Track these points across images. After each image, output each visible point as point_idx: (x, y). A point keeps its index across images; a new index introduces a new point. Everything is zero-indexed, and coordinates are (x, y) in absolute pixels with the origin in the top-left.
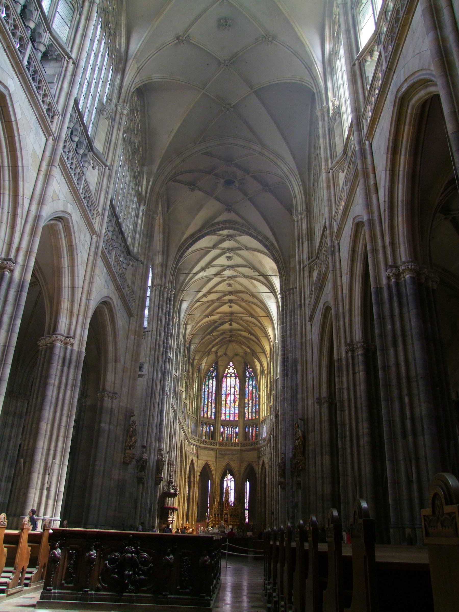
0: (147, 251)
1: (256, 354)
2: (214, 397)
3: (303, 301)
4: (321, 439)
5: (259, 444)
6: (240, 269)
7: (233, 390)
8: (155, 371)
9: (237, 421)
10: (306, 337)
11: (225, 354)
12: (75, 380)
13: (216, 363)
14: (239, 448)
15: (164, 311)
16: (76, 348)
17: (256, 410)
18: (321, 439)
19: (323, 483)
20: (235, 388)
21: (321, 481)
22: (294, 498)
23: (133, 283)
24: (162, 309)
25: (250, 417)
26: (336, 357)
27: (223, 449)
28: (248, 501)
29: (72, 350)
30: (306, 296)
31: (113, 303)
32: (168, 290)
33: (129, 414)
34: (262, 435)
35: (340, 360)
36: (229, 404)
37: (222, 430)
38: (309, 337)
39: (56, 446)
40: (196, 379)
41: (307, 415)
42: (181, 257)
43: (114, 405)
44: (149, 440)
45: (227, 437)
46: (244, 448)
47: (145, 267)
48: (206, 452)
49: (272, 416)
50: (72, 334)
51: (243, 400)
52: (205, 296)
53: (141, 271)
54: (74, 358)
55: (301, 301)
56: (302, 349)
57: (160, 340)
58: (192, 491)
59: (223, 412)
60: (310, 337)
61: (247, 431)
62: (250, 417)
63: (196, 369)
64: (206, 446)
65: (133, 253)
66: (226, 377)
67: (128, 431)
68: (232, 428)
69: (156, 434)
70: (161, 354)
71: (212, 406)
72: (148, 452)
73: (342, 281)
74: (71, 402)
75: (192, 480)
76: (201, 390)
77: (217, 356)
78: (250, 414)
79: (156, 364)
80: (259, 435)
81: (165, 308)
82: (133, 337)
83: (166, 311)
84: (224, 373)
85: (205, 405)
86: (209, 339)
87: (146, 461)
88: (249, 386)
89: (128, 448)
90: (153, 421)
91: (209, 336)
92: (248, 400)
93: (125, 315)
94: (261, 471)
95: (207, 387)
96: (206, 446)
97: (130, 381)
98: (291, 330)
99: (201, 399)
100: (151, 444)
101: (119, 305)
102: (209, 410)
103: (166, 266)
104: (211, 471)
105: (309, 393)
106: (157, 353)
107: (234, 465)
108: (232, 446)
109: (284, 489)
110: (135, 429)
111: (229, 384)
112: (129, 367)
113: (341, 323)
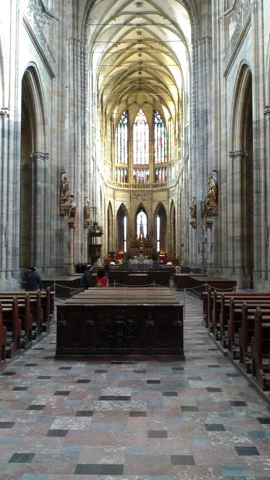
0: (61, 6)
1: (165, 102)
3: (218, 56)
4: (233, 189)
6: (149, 16)
7: (143, 136)
8: (76, 126)
9: (148, 165)
10: (220, 93)
11: (136, 102)
12: (16, 149)
13: (127, 112)
14: (151, 189)
15: (79, 65)
16: (12, 118)
18: (233, 189)
19: (233, 227)
21: (231, 225)
22: (204, 235)
23: (51, 42)
24: (77, 64)
25: (160, 162)
26: (254, 119)
27: (137, 191)
29: (9, 121)
30: (221, 50)
31: (37, 66)
32: (82, 43)
33: (60, 172)
34: (171, 177)
35: (258, 122)
38: (223, 93)
39: (8, 210)
40: (109, 127)
41: (220, 167)
42: (91, 6)
43: (47, 165)
44: (76, 190)
45: (139, 180)
46: (154, 189)
47: (61, 25)
49: (181, 161)
50: (6, 106)
51: (153, 146)
52: (115, 45)
53: (57, 29)
54: (12, 129)
55: (216, 55)
56: (216, 104)
57: (77, 95)
58: (110, 227)
60: (225, 93)
61: (157, 174)
63: (108, 118)
64: (121, 188)
65: (47, 9)
66: (136, 123)
67: (61, 187)
69: (81, 184)
70: (80, 109)
72: (76, 200)
73: (263, 42)
74: (15, 170)
77: (127, 104)
79: (76, 119)
80: (168, 177)
81: (79, 63)
82: (56, 98)
83: (81, 66)
86: (120, 88)
87: (75, 209)
89: (63, 201)
90: (78, 172)
91: (119, 86)
93: (48, 76)
96: (121, 188)
97: (58, 141)
98: (202, 80)
99: (114, 146)
100: (77, 193)
101: (42, 68)
103: (77, 17)
105: (222, 146)
106: (76, 108)
108: (144, 187)
109: (195, 228)
110: (67, 185)
112: (56, 128)
113: (261, 86)
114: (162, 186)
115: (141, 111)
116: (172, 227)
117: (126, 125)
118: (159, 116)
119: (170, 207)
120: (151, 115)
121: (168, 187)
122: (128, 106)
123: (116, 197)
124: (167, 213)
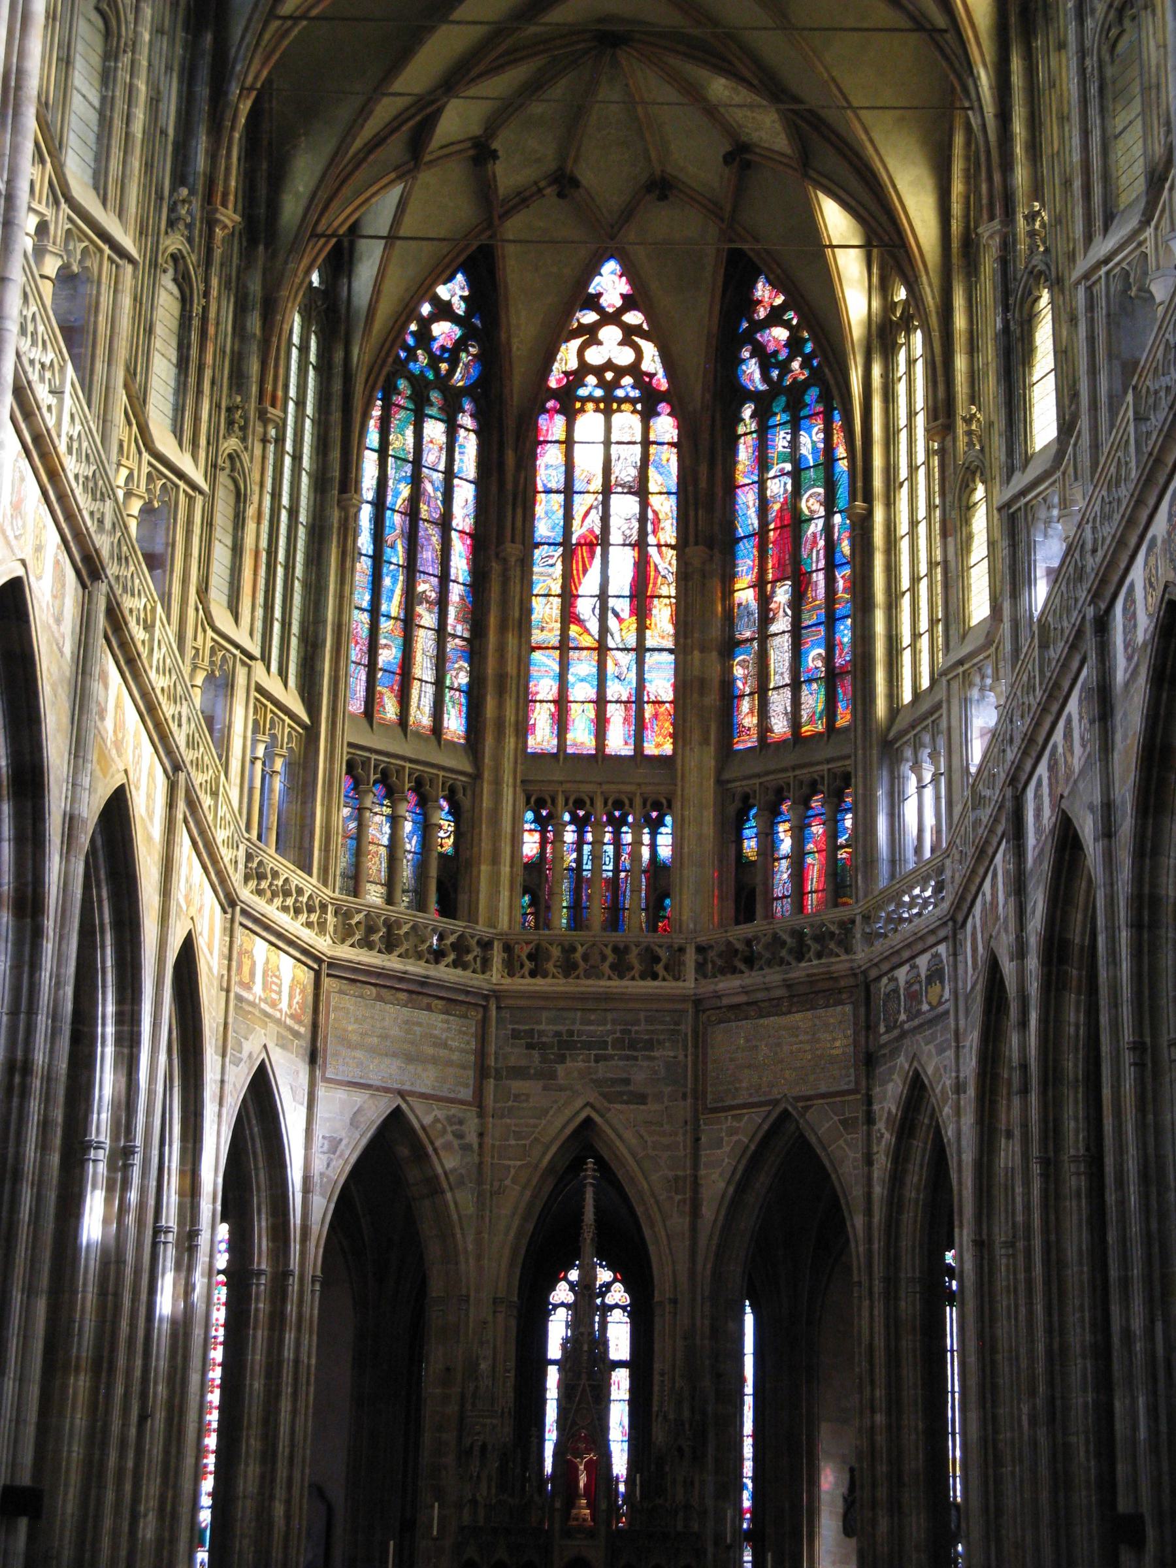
2: (460, 565)
7: (624, 507)
11: (564, 182)
14: (689, 984)
17: (829, 659)
20: (641, 490)
25: (780, 726)
28: (748, 1468)
36: (593, 626)
37: (530, 845)
45: (576, 908)
48: (392, 1016)
58: (257, 1356)
59: (544, 687)
61: (750, 846)
62: (780, 726)
64: (392, 962)
75: (262, 1262)
76: (349, 481)
77: (484, 191)
84: (546, 370)
85: (385, 625)
92: (761, 585)
94: (896, 1179)
95: (398, 474)
96: (392, 962)
102: (423, 669)
104: (433, 1187)
107: (639, 1141)
108: (620, 969)
111: (588, 461)
114: (800, 954)
115: (610, 284)
116: (911, 1375)
117: (468, 406)
118: (781, 334)
119: (882, 1162)
120: (699, 315)
121: (861, 954)
122: (491, 206)
123: (331, 1045)
124: (859, 1221)
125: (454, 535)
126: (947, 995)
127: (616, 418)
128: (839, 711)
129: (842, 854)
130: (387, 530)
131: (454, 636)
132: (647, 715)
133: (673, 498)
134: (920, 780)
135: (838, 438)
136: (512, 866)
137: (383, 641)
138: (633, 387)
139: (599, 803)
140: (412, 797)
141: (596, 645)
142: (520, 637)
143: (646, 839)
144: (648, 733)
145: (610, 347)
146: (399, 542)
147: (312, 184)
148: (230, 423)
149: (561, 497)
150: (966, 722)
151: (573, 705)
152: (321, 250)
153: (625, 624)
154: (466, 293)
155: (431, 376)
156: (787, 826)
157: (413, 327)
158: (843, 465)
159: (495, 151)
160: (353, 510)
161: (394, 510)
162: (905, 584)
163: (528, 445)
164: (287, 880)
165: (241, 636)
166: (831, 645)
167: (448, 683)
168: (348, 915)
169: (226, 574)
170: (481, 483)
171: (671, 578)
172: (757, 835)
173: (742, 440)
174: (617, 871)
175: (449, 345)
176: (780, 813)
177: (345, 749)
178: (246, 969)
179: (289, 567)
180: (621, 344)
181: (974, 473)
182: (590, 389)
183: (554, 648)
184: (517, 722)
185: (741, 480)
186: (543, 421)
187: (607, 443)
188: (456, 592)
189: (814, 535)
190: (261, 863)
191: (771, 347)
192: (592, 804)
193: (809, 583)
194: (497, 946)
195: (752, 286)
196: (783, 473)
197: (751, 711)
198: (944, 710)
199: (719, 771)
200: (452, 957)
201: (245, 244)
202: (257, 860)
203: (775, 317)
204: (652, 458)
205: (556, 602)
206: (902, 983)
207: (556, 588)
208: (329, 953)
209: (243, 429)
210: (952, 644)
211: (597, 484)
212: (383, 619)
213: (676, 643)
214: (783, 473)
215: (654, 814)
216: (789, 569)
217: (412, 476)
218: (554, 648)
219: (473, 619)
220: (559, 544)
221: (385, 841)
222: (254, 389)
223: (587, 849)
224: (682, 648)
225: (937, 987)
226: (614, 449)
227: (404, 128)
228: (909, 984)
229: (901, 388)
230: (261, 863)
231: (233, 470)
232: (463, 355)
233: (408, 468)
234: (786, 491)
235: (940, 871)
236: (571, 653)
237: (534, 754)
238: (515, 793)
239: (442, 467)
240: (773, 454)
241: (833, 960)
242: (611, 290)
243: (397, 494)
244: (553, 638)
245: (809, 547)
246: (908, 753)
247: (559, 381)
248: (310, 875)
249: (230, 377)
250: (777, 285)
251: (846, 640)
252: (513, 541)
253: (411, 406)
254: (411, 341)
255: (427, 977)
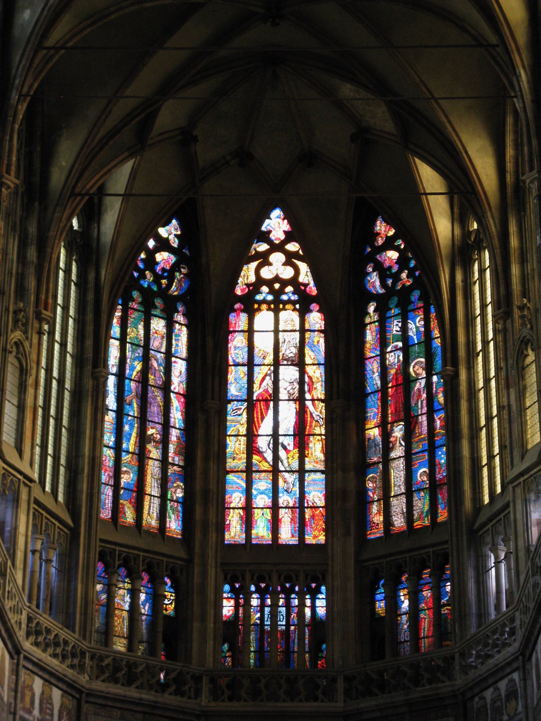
2: (177, 416)
5: (466, 668)
7: (289, 374)
11: (243, 157)
14: (339, 704)
17: (431, 475)
20: (300, 362)
25: (399, 522)
37: (228, 608)
45: (260, 651)
59: (236, 498)
61: (381, 606)
62: (399, 522)
64: (132, 693)
68: (288, 593)
71: (164, 462)
78: (398, 505)
85: (126, 458)
88: (383, 342)
96: (132, 693)
102: (152, 487)
111: (264, 343)
117: (181, 308)
118: (393, 255)
121: (460, 681)
125: (172, 395)
126: (520, 709)
127: (283, 315)
128: (440, 510)
129: (445, 611)
130: (126, 393)
131: (173, 465)
132: (307, 516)
133: (322, 368)
134: (496, 557)
135: (434, 324)
136: (215, 623)
137: (124, 469)
138: (294, 293)
139: (275, 578)
140: (145, 576)
141: (271, 469)
142: (218, 464)
143: (308, 602)
144: (308, 529)
145: (277, 267)
146: (134, 401)
147: (71, 160)
148: (16, 321)
149: (245, 369)
150: (527, 515)
151: (256, 510)
152: (78, 204)
153: (291, 454)
154: (179, 233)
155: (155, 289)
156: (405, 591)
157: (143, 256)
158: (437, 342)
159: (196, 136)
160: (102, 380)
161: (131, 380)
162: (483, 422)
163: (223, 334)
164: (56, 635)
165: (24, 467)
166: (432, 464)
167: (169, 497)
168: (101, 658)
169: (13, 424)
170: (190, 360)
171: (322, 422)
172: (385, 598)
173: (368, 327)
174: (288, 625)
175: (168, 268)
176: (401, 583)
177: (98, 543)
178: (28, 699)
179: (58, 419)
180: (284, 264)
181: (526, 344)
182: (264, 295)
183: (242, 471)
184: (217, 522)
185: (369, 354)
186: (232, 317)
187: (276, 331)
188: (174, 434)
189: (419, 390)
190: (38, 624)
191: (387, 264)
192: (270, 578)
193: (417, 422)
194: (205, 679)
195: (374, 224)
196: (396, 349)
197: (379, 512)
198: (511, 509)
199: (358, 554)
200: (174, 687)
201: (25, 201)
202: (35, 622)
203: (389, 244)
204: (307, 341)
205: (243, 440)
206: (489, 701)
207: (243, 430)
208: (88, 686)
209: (25, 325)
210: (515, 462)
211: (270, 359)
212: (124, 454)
213: (326, 467)
214: (396, 349)
215: (314, 585)
216: (402, 414)
217: (143, 356)
218: (242, 471)
219: (185, 453)
220: (245, 401)
221: (127, 607)
222: (32, 298)
223: (267, 610)
224: (330, 469)
225: (514, 703)
226: (281, 335)
227: (134, 122)
228: (493, 701)
229: (477, 288)
230: (38, 624)
231: (18, 353)
232: (177, 274)
233: (140, 351)
234: (399, 360)
235: (512, 620)
236: (254, 475)
237: (230, 545)
238: (216, 572)
239: (163, 350)
240: (390, 336)
241: (440, 685)
242: (277, 229)
243: (133, 368)
244: (241, 464)
245: (415, 398)
246: (489, 539)
247: (242, 290)
248: (74, 631)
249: (16, 292)
250: (389, 222)
251: (443, 461)
252: (213, 399)
253: (142, 309)
254: (141, 266)
255: (156, 702)
